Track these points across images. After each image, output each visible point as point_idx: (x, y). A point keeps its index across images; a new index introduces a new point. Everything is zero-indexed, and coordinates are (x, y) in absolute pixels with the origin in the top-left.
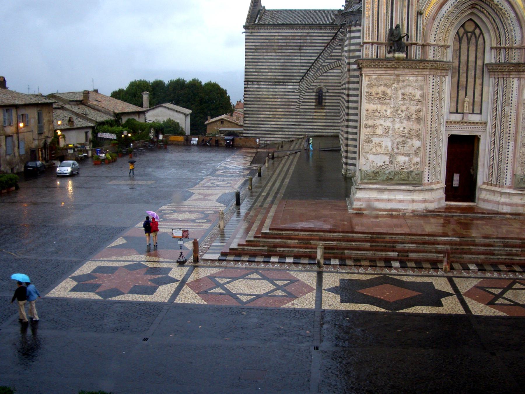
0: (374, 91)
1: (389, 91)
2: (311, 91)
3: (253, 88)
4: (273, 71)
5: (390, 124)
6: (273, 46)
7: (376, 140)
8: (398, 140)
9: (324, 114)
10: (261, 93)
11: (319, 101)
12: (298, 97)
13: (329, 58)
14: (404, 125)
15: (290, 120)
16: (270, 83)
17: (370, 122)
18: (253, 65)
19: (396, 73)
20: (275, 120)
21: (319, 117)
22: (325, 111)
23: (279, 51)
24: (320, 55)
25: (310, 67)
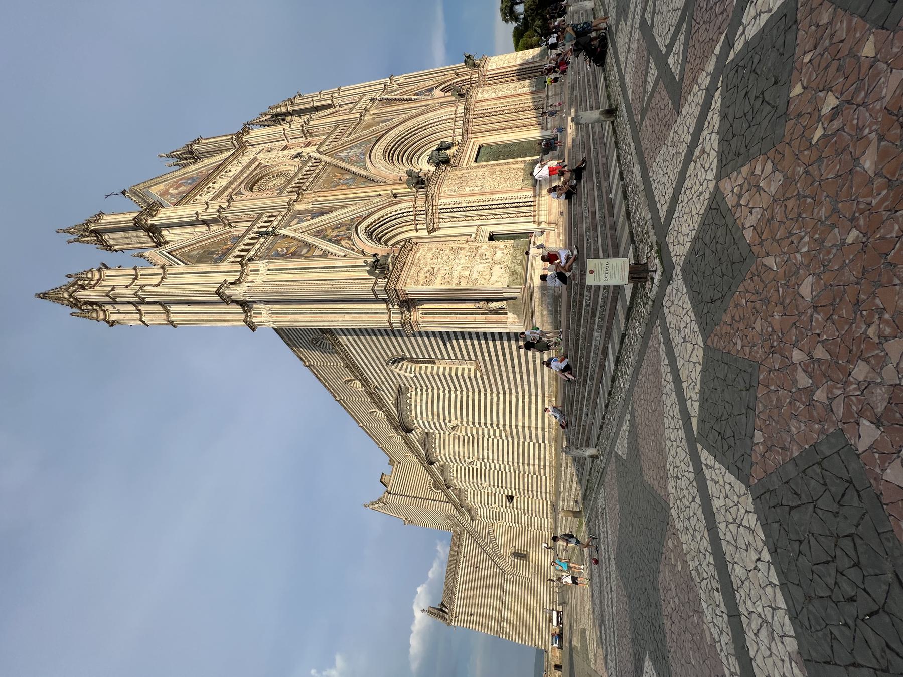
0: (422, 280)
1: (426, 270)
2: (513, 563)
3: (506, 629)
4: (492, 601)
5: (461, 266)
7: (475, 276)
8: (478, 260)
9: (534, 553)
10: (512, 619)
11: (523, 557)
12: (518, 578)
13: (486, 541)
14: (463, 256)
15: (539, 590)
16: (503, 607)
17: (455, 281)
18: (485, 623)
19: (409, 264)
20: (538, 608)
21: (537, 558)
24: (483, 548)
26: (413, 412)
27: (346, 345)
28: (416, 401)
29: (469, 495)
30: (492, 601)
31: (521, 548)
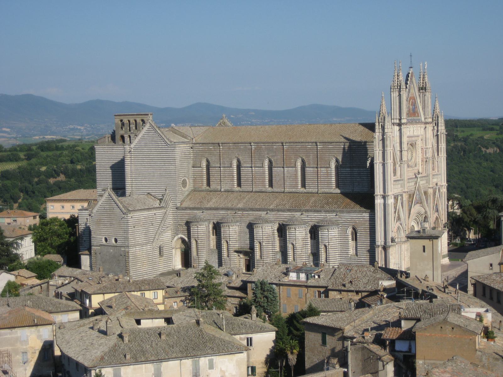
6: (140, 223)
13: (164, 226)
20: (143, 268)
22: (163, 258)
23: (143, 226)
25: (156, 233)
26: (331, 230)
27: (362, 214)
28: (335, 231)
29: (234, 227)
30: (141, 238)
31: (165, 250)
